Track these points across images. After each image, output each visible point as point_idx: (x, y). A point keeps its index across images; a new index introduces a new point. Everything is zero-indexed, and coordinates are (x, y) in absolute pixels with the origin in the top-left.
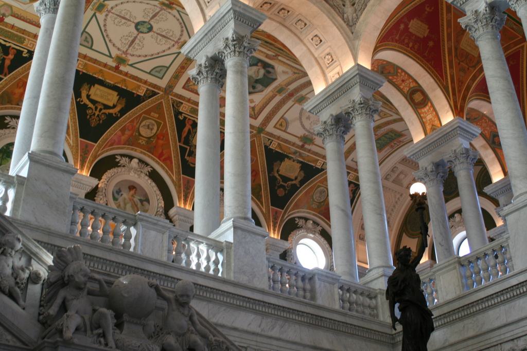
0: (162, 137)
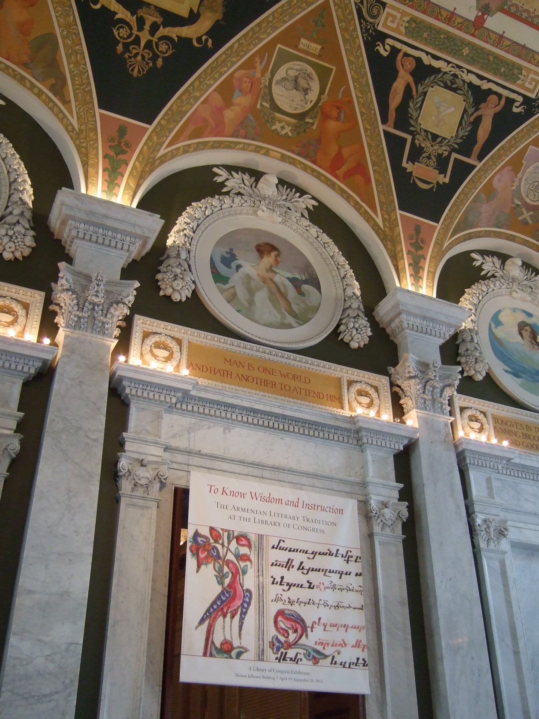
0: (335, 113)
